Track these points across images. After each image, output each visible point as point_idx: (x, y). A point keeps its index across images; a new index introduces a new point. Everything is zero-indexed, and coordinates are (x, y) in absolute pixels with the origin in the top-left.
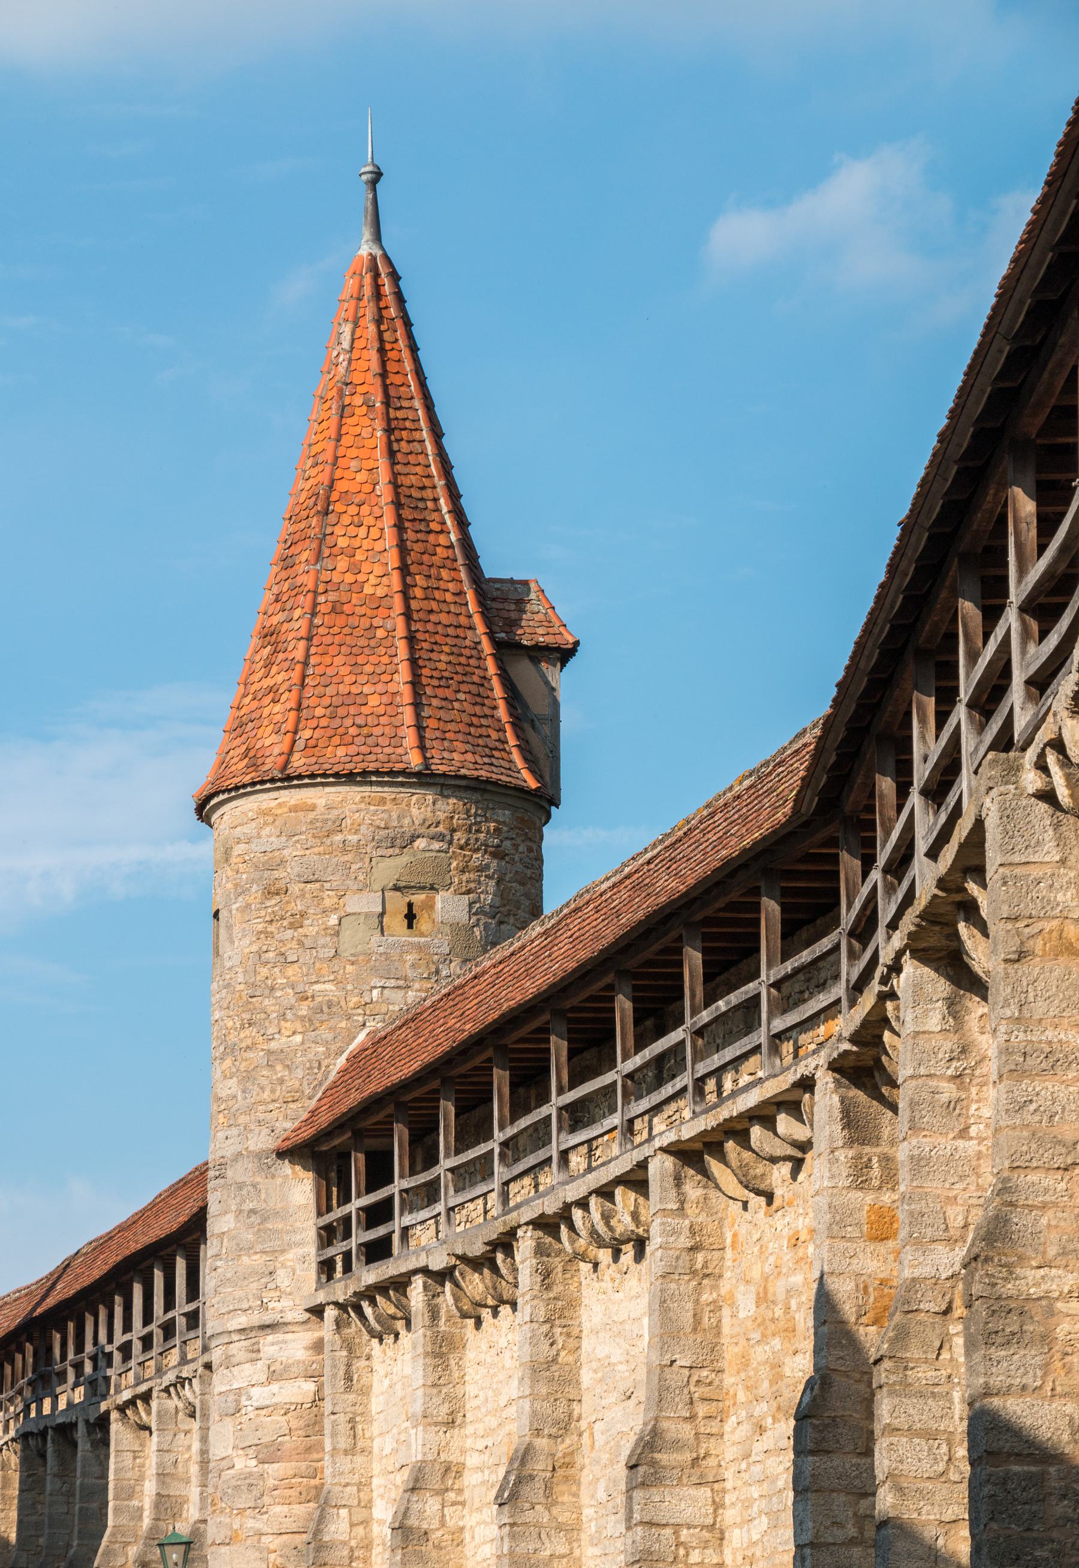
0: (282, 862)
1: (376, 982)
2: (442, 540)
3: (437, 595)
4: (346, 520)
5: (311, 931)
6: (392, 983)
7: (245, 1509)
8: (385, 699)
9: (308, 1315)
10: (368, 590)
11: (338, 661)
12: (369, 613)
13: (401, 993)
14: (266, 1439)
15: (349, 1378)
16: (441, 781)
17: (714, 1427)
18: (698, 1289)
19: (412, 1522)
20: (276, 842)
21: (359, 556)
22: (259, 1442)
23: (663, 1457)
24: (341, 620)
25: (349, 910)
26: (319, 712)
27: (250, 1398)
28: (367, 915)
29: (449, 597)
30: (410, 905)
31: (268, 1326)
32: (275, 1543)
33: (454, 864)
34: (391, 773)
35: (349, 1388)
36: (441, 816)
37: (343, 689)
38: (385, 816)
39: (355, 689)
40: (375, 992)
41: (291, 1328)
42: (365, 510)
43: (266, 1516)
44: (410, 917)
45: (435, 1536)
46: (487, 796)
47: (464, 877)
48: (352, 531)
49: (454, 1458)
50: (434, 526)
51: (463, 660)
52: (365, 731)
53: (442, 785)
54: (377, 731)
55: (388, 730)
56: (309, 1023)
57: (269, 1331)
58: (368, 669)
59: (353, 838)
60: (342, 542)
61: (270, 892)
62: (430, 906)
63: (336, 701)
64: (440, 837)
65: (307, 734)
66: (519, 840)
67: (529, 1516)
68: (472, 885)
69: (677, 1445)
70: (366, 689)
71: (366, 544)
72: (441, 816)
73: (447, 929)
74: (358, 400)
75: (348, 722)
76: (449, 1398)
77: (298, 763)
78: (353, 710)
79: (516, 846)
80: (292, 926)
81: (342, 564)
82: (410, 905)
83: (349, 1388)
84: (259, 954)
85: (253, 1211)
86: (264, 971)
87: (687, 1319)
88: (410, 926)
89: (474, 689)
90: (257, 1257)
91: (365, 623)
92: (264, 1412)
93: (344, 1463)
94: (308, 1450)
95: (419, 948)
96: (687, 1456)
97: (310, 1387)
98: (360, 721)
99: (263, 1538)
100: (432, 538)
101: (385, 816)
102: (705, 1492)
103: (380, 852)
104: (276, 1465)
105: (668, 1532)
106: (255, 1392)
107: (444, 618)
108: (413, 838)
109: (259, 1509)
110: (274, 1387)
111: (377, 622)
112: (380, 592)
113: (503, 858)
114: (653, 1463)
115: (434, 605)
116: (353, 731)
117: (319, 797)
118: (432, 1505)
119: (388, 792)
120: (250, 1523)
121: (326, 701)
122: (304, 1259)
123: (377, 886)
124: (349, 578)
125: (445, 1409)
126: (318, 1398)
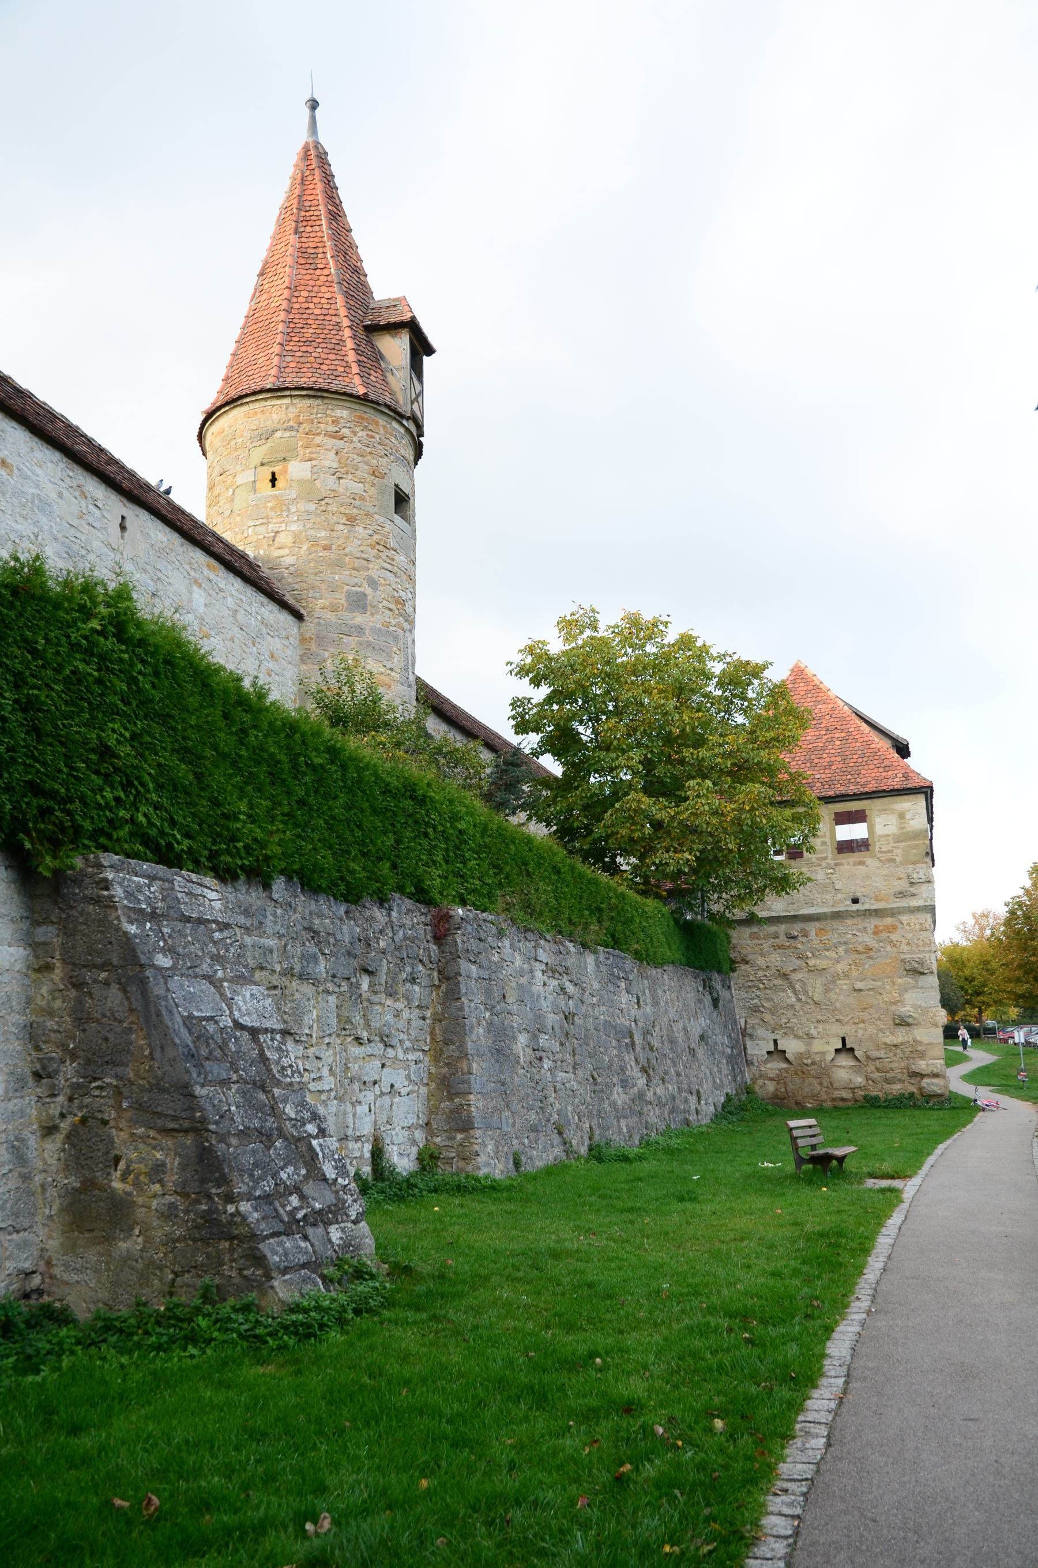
2: (325, 272)
3: (314, 300)
4: (270, 274)
6: (260, 521)
10: (273, 305)
12: (269, 316)
13: (265, 527)
16: (288, 393)
25: (238, 484)
28: (246, 484)
29: (323, 301)
30: (273, 474)
33: (300, 443)
34: (254, 393)
36: (291, 416)
38: (257, 422)
44: (273, 480)
46: (326, 401)
47: (308, 451)
51: (325, 331)
53: (291, 396)
59: (240, 440)
62: (285, 471)
64: (291, 428)
66: (357, 429)
68: (314, 456)
72: (291, 416)
73: (295, 484)
79: (355, 433)
81: (264, 297)
82: (273, 474)
88: (274, 486)
91: (267, 322)
95: (276, 497)
100: (318, 272)
101: (257, 422)
103: (254, 444)
107: (317, 312)
108: (274, 431)
113: (341, 439)
115: (311, 306)
123: (253, 466)
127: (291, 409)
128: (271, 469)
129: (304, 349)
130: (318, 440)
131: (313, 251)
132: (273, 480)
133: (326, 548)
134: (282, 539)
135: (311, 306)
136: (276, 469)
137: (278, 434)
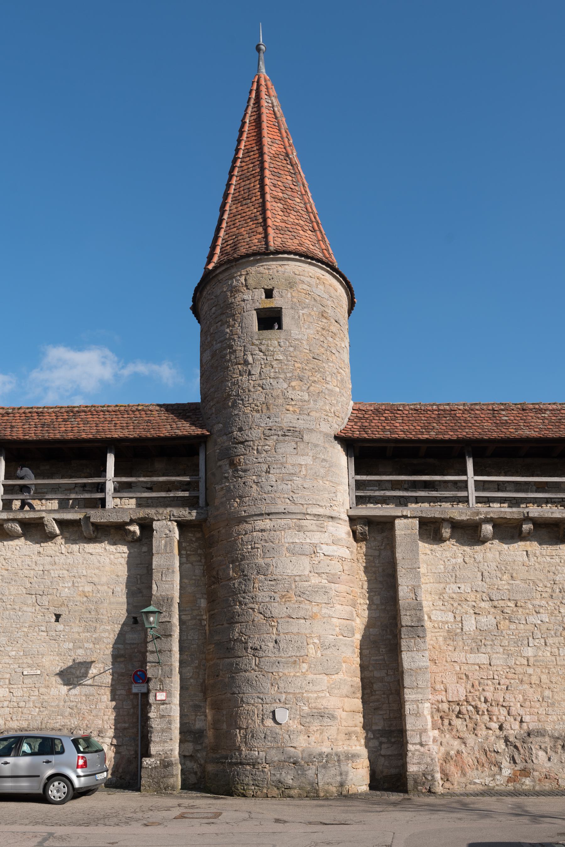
7: (321, 603)
9: (347, 519)
14: (333, 572)
22: (328, 572)
27: (321, 549)
31: (332, 517)
41: (340, 522)
43: (333, 609)
57: (331, 519)
90: (327, 483)
92: (329, 558)
99: (332, 619)
104: (337, 585)
106: (323, 546)
110: (335, 547)
120: (324, 611)
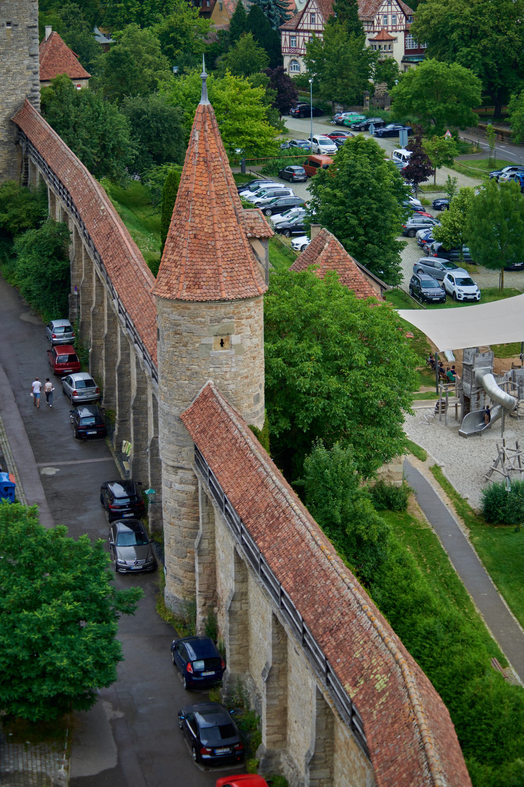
0: (180, 325)
1: (212, 366)
3: (229, 229)
4: (198, 204)
5: (190, 348)
8: (212, 271)
10: (206, 230)
11: (197, 256)
15: (207, 502)
17: (331, 753)
18: (327, 719)
19: (232, 609)
20: (178, 318)
21: (203, 217)
23: (316, 762)
24: (197, 241)
26: (191, 275)
29: (232, 229)
32: (185, 530)
35: (207, 505)
37: (199, 267)
39: (203, 267)
40: (211, 369)
42: (204, 200)
44: (222, 344)
45: (239, 613)
48: (200, 208)
49: (244, 590)
50: (227, 203)
52: (206, 283)
54: (210, 283)
55: (214, 283)
56: (190, 378)
58: (207, 260)
60: (197, 212)
61: (176, 334)
62: (228, 340)
63: (196, 271)
65: (187, 283)
67: (272, 686)
69: (321, 759)
70: (207, 267)
71: (205, 213)
74: (201, 159)
75: (200, 280)
76: (242, 575)
77: (185, 295)
78: (202, 275)
80: (184, 346)
83: (207, 505)
84: (174, 352)
85: (173, 432)
86: (175, 358)
87: (324, 726)
89: (241, 261)
91: (205, 243)
93: (207, 527)
94: (194, 506)
96: (323, 761)
97: (193, 488)
98: (204, 279)
100: (227, 208)
102: (328, 770)
105: (317, 781)
107: (231, 237)
109: (180, 520)
111: (209, 242)
112: (210, 231)
114: (313, 764)
116: (202, 283)
117: (192, 306)
118: (238, 604)
119: (214, 305)
121: (193, 271)
122: (190, 450)
124: (200, 226)
125: (241, 578)
126: (197, 490)
127: (232, 307)
128: (220, 338)
129: (231, 266)
130: (243, 321)
131: (222, 193)
132: (222, 344)
133: (247, 377)
134: (228, 376)
135: (228, 233)
136: (224, 338)
137: (226, 320)
